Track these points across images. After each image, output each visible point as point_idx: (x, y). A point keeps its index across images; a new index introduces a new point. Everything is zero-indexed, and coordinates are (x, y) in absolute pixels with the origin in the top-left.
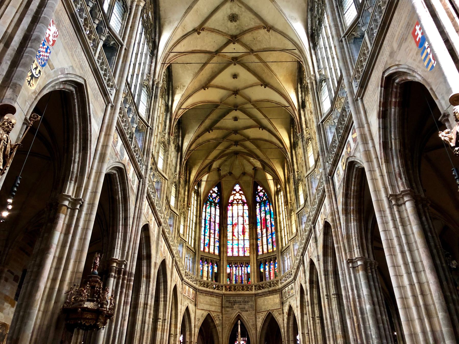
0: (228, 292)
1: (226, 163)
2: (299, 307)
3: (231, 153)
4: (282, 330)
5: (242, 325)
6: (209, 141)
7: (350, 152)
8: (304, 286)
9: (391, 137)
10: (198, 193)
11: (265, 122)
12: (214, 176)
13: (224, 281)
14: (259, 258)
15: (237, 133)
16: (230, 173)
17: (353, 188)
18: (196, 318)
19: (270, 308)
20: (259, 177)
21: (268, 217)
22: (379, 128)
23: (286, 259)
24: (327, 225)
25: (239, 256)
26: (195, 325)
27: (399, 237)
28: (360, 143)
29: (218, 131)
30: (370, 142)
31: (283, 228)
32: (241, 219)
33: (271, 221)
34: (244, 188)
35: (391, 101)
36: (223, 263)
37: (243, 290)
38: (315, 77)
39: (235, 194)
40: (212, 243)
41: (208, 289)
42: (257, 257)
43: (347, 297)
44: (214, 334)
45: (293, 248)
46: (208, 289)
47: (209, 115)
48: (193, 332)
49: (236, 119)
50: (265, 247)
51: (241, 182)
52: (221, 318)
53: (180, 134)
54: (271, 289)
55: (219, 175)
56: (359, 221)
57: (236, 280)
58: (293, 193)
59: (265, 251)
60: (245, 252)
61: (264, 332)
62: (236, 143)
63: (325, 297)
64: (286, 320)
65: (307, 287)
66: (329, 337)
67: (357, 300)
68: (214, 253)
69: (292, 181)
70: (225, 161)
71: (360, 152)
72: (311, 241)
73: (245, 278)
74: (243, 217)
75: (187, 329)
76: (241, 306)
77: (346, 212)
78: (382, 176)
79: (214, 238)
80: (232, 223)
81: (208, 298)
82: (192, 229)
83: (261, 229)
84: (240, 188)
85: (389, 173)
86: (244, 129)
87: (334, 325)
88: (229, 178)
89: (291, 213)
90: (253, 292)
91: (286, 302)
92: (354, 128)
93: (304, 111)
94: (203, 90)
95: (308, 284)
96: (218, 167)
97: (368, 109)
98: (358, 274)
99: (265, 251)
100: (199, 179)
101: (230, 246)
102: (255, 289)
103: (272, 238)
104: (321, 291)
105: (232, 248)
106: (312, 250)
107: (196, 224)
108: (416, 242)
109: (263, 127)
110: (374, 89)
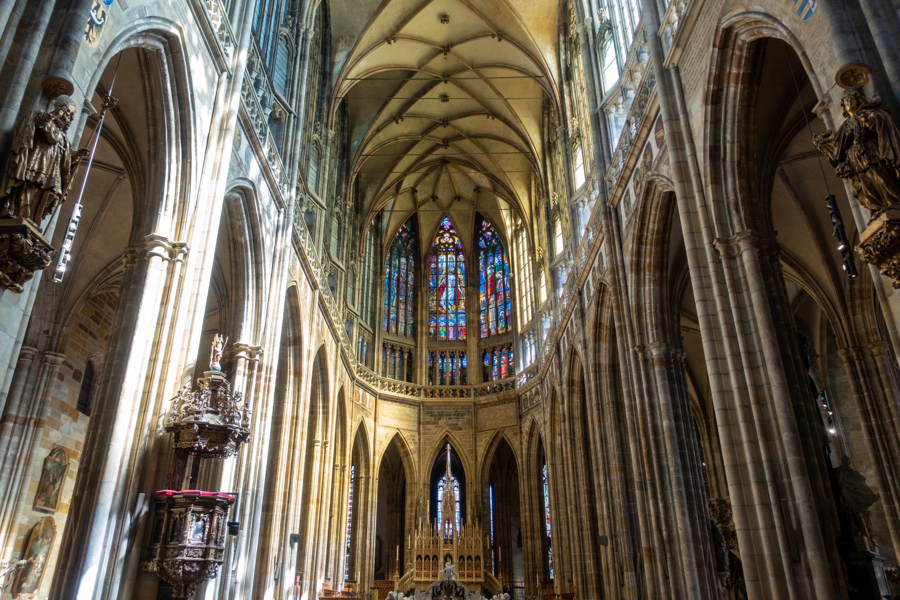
0: (429, 399)
1: (427, 179)
2: (548, 424)
3: (436, 160)
4: (519, 460)
5: (453, 451)
6: (396, 138)
7: (651, 162)
8: (558, 388)
9: (725, 138)
10: (377, 232)
11: (498, 105)
14: (482, 344)
15: (448, 124)
16: (434, 198)
17: (651, 227)
18: (377, 439)
19: (499, 425)
21: (498, 275)
22: (706, 121)
23: (528, 345)
24: (601, 289)
25: (447, 340)
26: (374, 452)
27: (727, 310)
28: (669, 148)
29: (412, 120)
30: (687, 147)
31: (524, 294)
32: (451, 277)
33: (503, 281)
34: (457, 223)
35: (730, 73)
36: (421, 351)
37: (454, 395)
38: (593, 24)
39: (442, 235)
40: (402, 319)
41: (395, 394)
42: (478, 343)
43: (633, 408)
44: (406, 465)
45: (542, 326)
47: (396, 91)
48: (371, 463)
49: (445, 98)
51: (452, 213)
52: (417, 440)
53: (346, 126)
55: (414, 200)
56: (659, 282)
58: (544, 234)
59: (493, 331)
61: (489, 462)
62: (446, 142)
63: (595, 408)
64: (525, 444)
65: (562, 390)
66: (598, 470)
67: (648, 412)
68: (405, 335)
69: (543, 212)
70: (425, 175)
71: (668, 163)
72: (573, 316)
74: (455, 273)
75: (362, 458)
76: (450, 422)
77: (638, 268)
78: (705, 206)
79: (406, 309)
80: (437, 284)
81: (395, 408)
82: (367, 294)
83: (486, 296)
84: (449, 224)
85: (718, 201)
86: (460, 117)
87: (607, 452)
88: (430, 205)
89: (540, 266)
90: (472, 399)
91: (527, 415)
92: (660, 121)
93: (569, 85)
94: (386, 43)
95: (565, 386)
96: (412, 185)
97: (687, 87)
98: (652, 371)
100: (378, 207)
102: (475, 396)
104: (587, 398)
106: (575, 331)
108: (754, 319)
109: (494, 114)
110: (701, 51)
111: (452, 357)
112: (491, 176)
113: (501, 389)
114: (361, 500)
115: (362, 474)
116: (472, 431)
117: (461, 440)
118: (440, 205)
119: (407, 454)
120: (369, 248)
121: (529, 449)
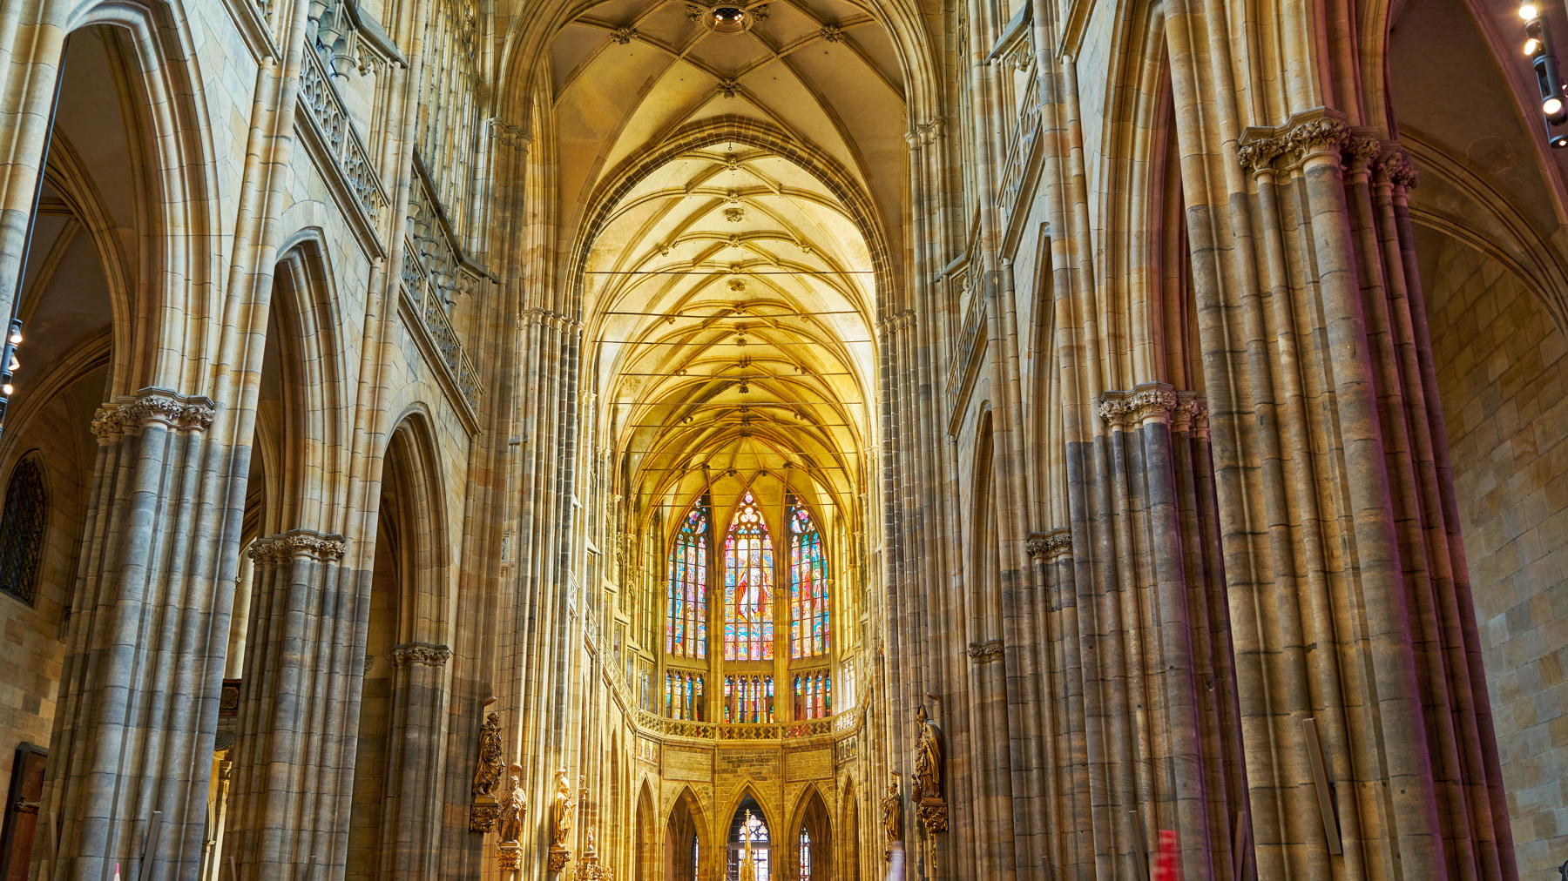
0: (726, 741)
12: (692, 482)
13: (718, 714)
20: (800, 479)
32: (755, 572)
34: (763, 502)
37: (758, 735)
40: (690, 634)
41: (684, 738)
46: (684, 738)
50: (807, 642)
54: (814, 738)
55: (706, 477)
57: (742, 712)
59: (807, 652)
60: (763, 649)
61: (799, 819)
62: (746, 420)
64: (840, 802)
73: (761, 707)
74: (761, 567)
75: (645, 820)
76: (752, 770)
79: (696, 620)
81: (684, 756)
83: (800, 601)
88: (727, 480)
90: (779, 740)
99: (807, 652)
101: (730, 637)
103: (823, 624)
105: (735, 642)
107: (655, 595)
111: (756, 682)
112: (805, 457)
113: (815, 731)
114: (646, 871)
115: (646, 840)
116: (778, 782)
117: (765, 792)
118: (740, 480)
119: (699, 811)
120: (648, 544)
121: (845, 808)
